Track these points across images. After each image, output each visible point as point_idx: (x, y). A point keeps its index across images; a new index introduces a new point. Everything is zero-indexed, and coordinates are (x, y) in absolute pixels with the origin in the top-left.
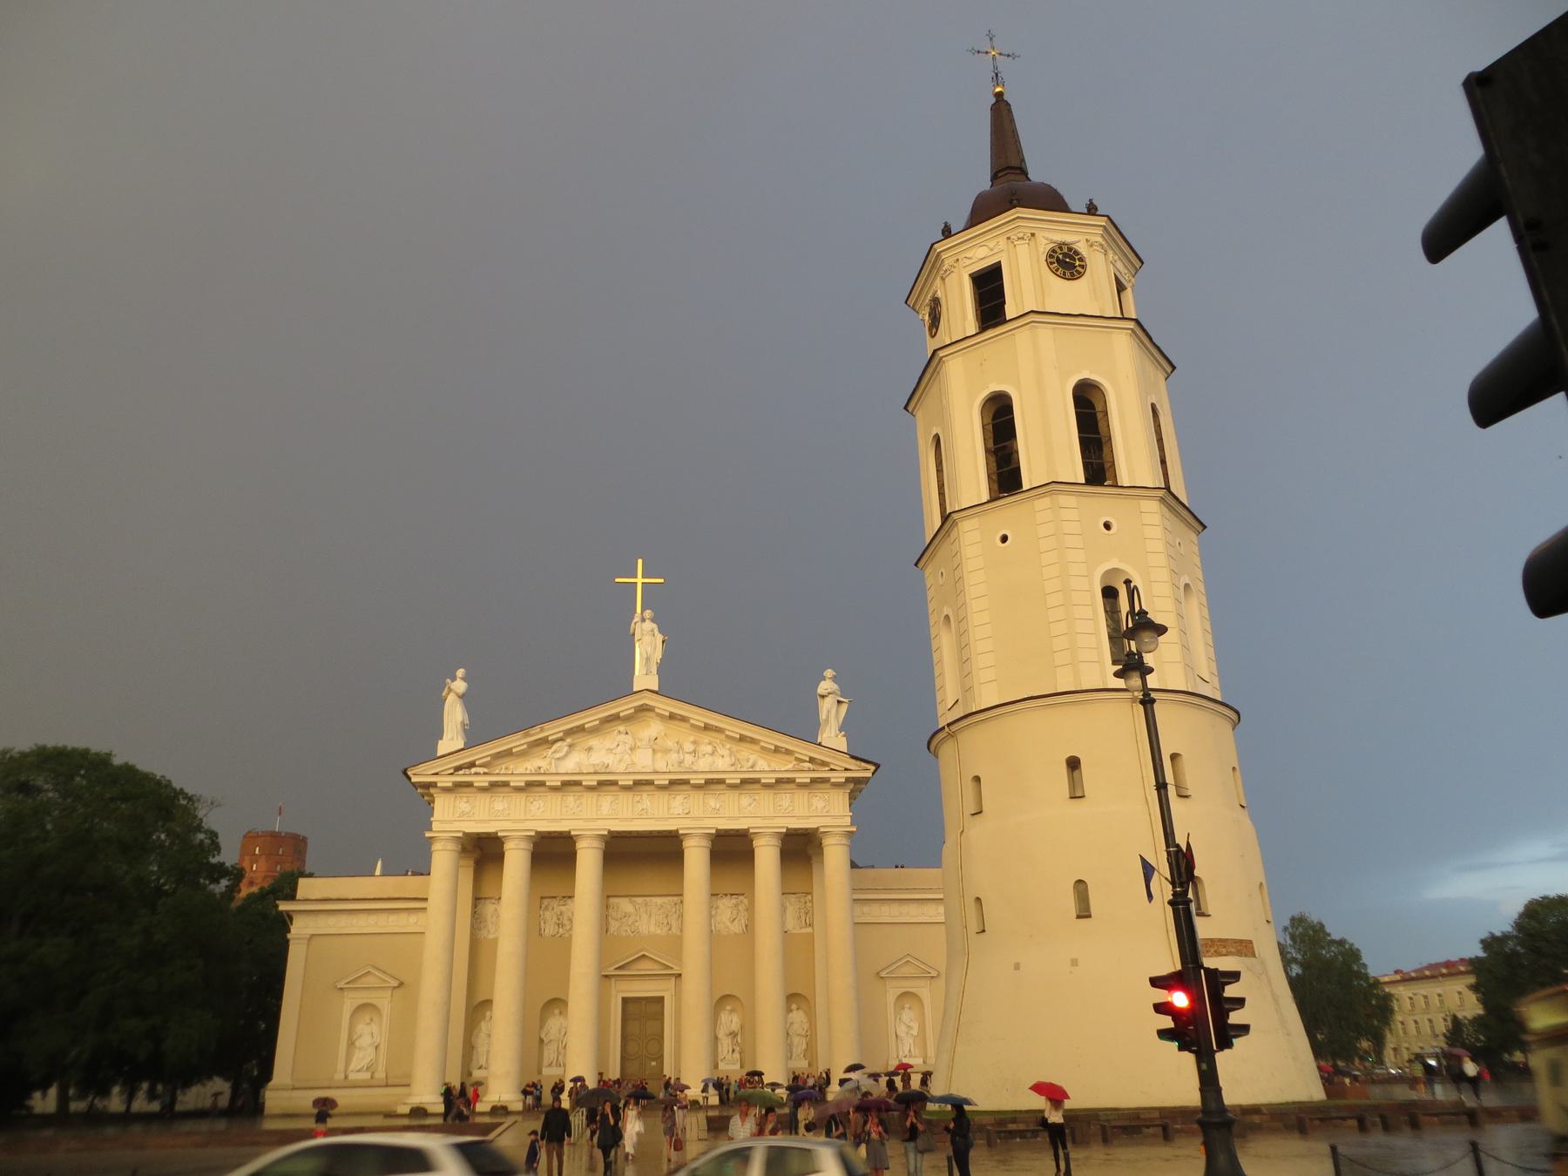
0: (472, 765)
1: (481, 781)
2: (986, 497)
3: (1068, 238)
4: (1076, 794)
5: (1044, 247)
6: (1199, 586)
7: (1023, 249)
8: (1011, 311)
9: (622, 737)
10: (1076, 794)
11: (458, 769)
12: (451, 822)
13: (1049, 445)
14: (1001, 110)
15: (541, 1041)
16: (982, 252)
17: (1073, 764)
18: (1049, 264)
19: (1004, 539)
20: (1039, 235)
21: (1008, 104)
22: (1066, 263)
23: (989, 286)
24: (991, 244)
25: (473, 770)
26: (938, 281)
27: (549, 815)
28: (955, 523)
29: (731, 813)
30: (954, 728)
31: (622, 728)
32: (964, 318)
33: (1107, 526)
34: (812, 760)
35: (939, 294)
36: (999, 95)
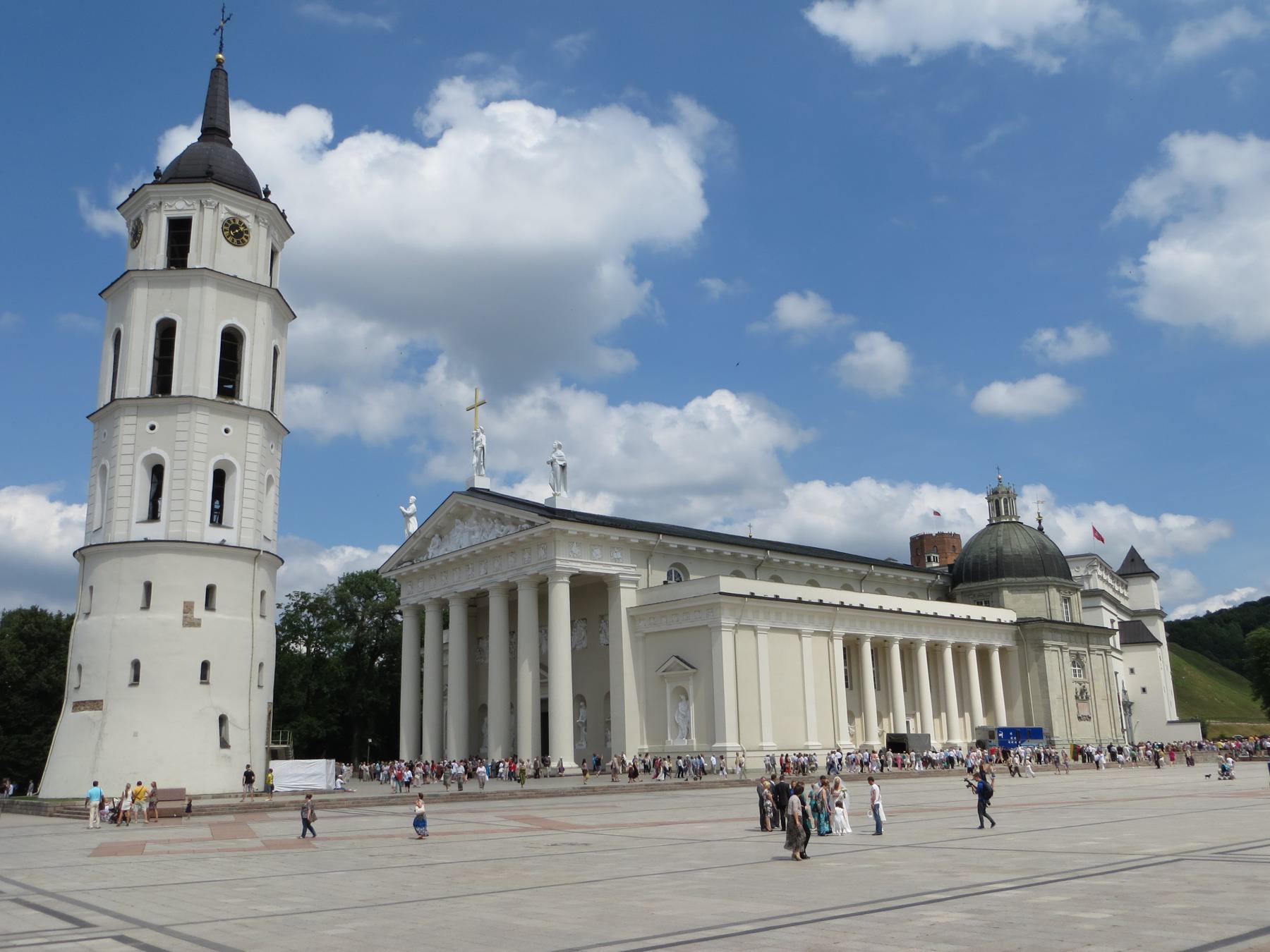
2: (147, 392)
3: (242, 213)
5: (224, 216)
6: (276, 482)
8: (192, 260)
13: (197, 369)
16: (180, 205)
18: (223, 231)
19: (152, 428)
20: (223, 207)
22: (236, 233)
26: (143, 209)
28: (119, 407)
32: (158, 252)
33: (226, 431)
36: (219, 62)
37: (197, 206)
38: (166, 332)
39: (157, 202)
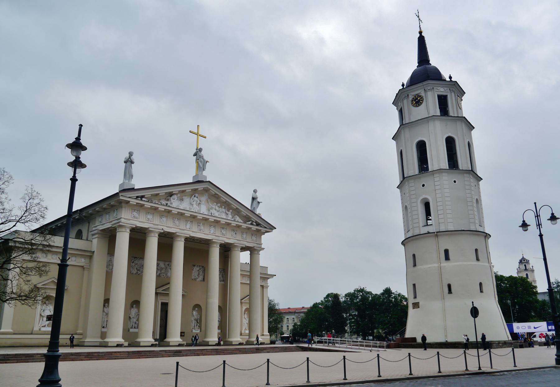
0: (142, 197)
1: (148, 205)
2: (448, 168)
4: (478, 259)
7: (453, 94)
8: (451, 114)
9: (195, 198)
10: (478, 259)
11: (137, 197)
12: (129, 220)
14: (421, 40)
15: (130, 318)
16: (442, 90)
17: (476, 250)
21: (423, 37)
23: (443, 101)
24: (446, 89)
25: (143, 199)
27: (168, 226)
29: (228, 238)
30: (438, 233)
31: (197, 195)
34: (256, 222)
35: (423, 94)
37: (448, 91)
38: (450, 143)
39: (431, 88)
